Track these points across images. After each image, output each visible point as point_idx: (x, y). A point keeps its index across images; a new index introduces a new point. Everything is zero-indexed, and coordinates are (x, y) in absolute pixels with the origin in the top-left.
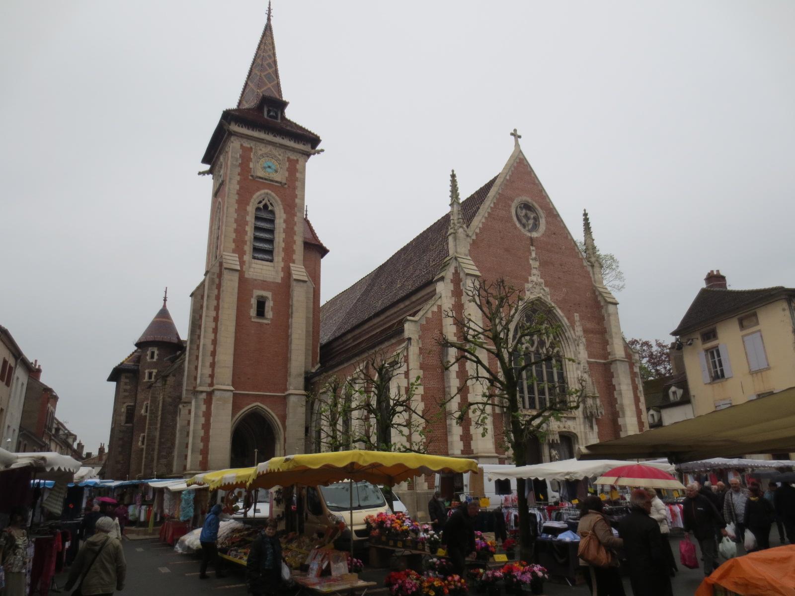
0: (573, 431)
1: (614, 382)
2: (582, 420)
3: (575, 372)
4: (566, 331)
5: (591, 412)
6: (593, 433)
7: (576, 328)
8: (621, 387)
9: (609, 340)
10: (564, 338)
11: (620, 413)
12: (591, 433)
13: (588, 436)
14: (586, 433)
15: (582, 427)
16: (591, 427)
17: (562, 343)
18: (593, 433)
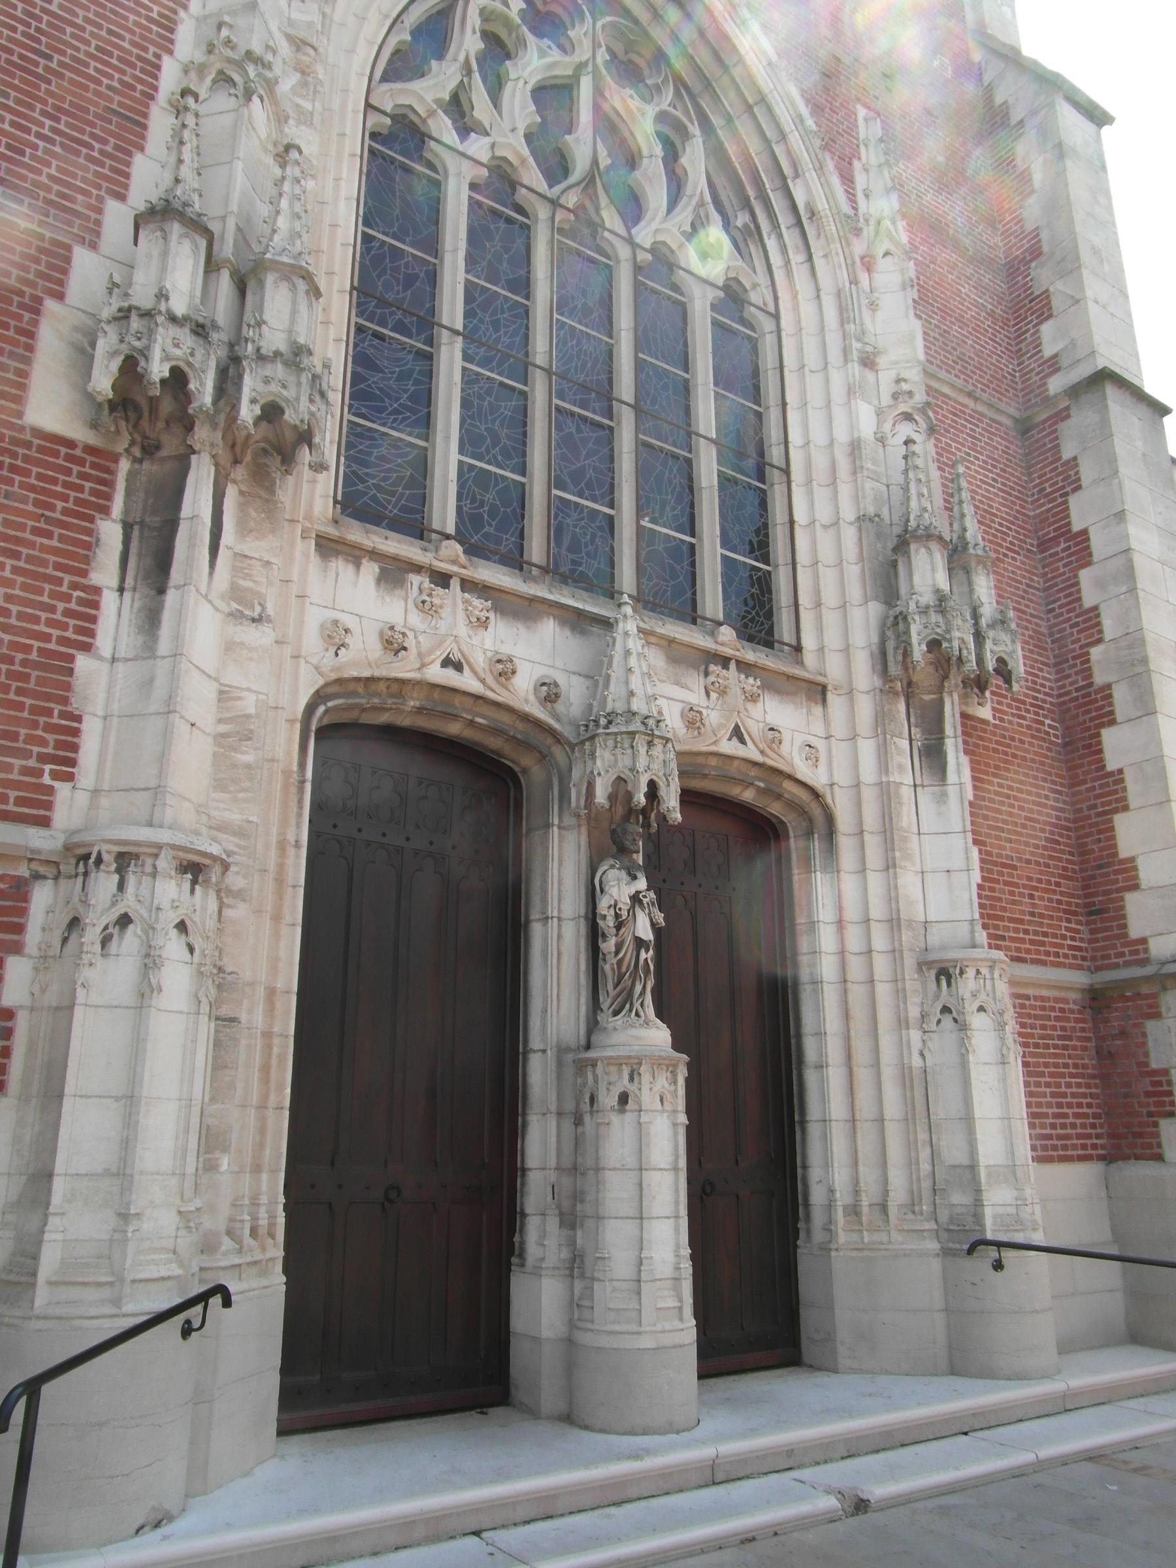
0: (803, 771)
1: (1082, 512)
2: (865, 708)
3: (839, 414)
4: (797, 175)
5: (934, 645)
6: (941, 799)
7: (860, 180)
8: (1132, 530)
9: (1059, 288)
10: (784, 219)
11: (1121, 697)
12: (924, 797)
13: (906, 817)
14: (887, 793)
15: (867, 749)
16: (932, 755)
17: (771, 244)
18: (942, 799)
